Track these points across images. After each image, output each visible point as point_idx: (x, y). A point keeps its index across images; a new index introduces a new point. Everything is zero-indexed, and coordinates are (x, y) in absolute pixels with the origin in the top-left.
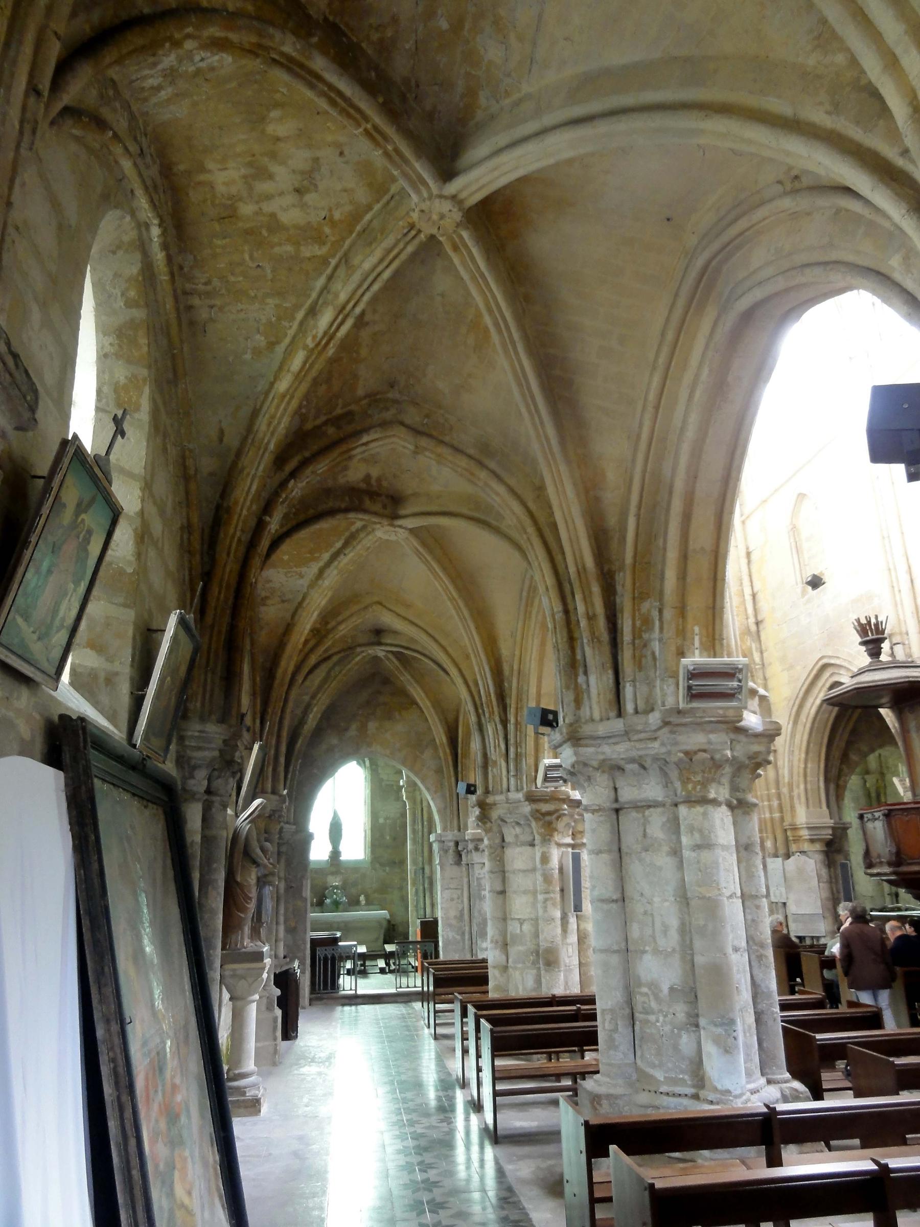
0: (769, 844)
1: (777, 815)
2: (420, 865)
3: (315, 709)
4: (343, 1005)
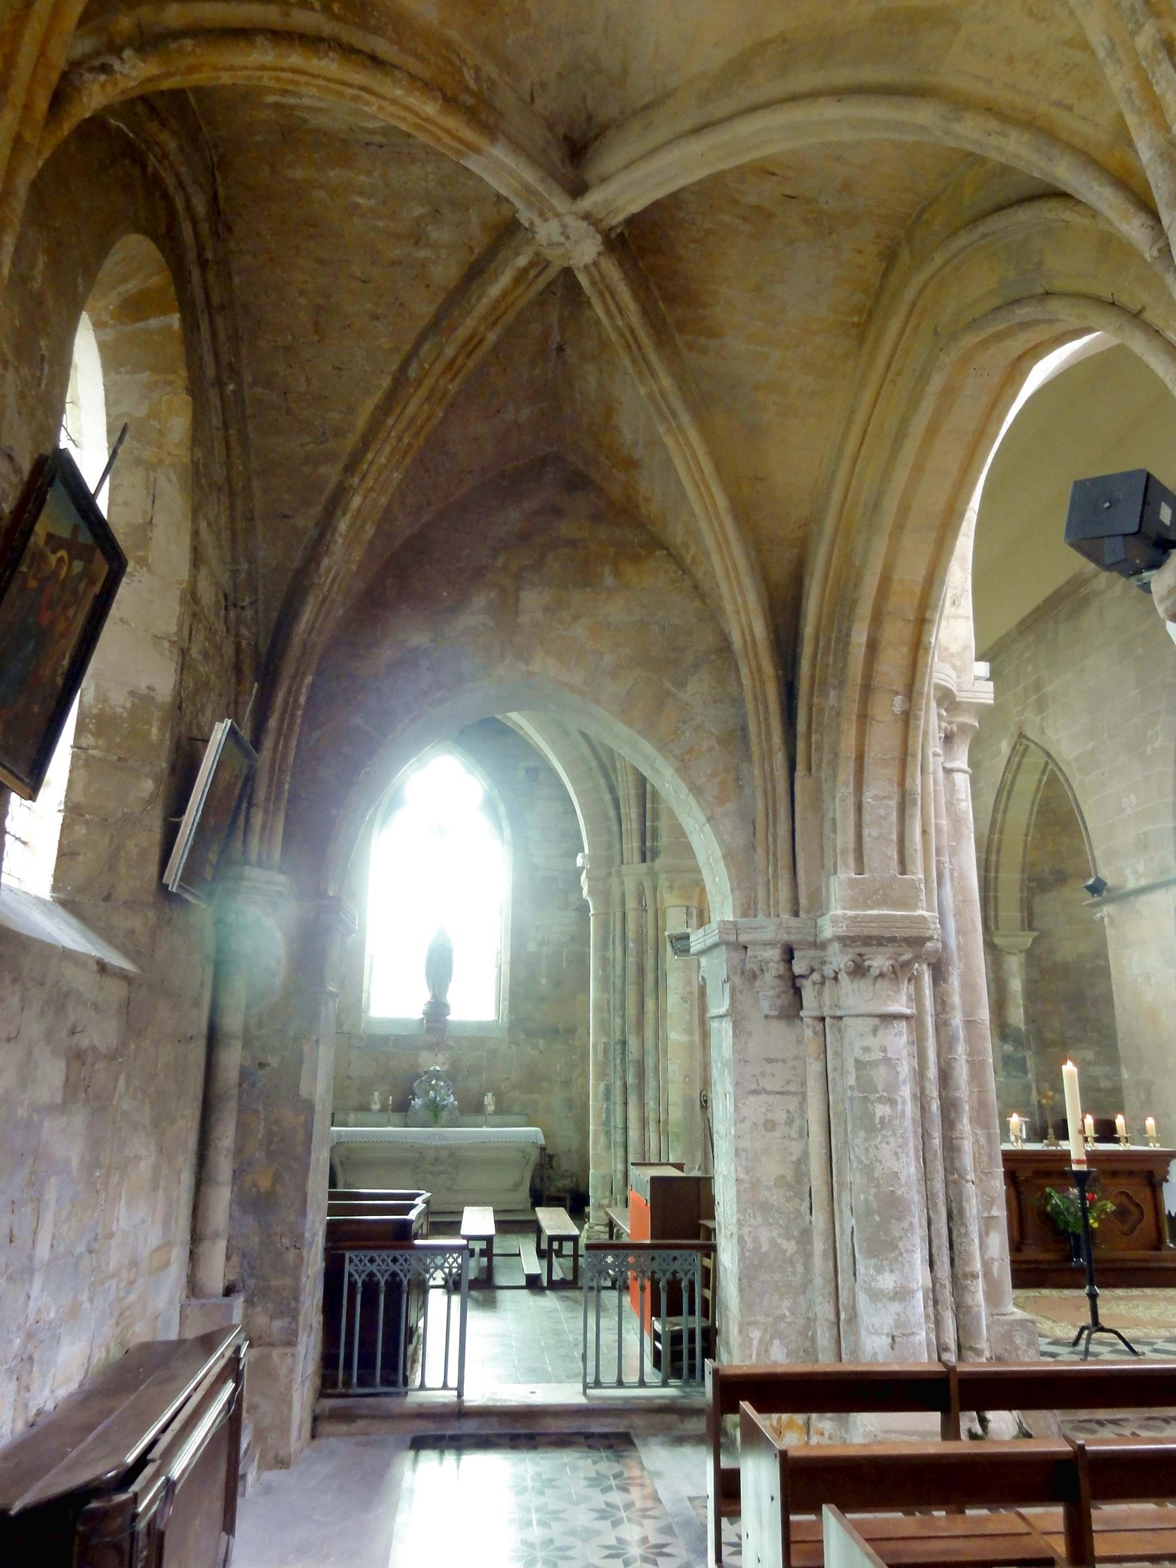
2: (618, 1036)
3: (356, 502)
4: (419, 1444)
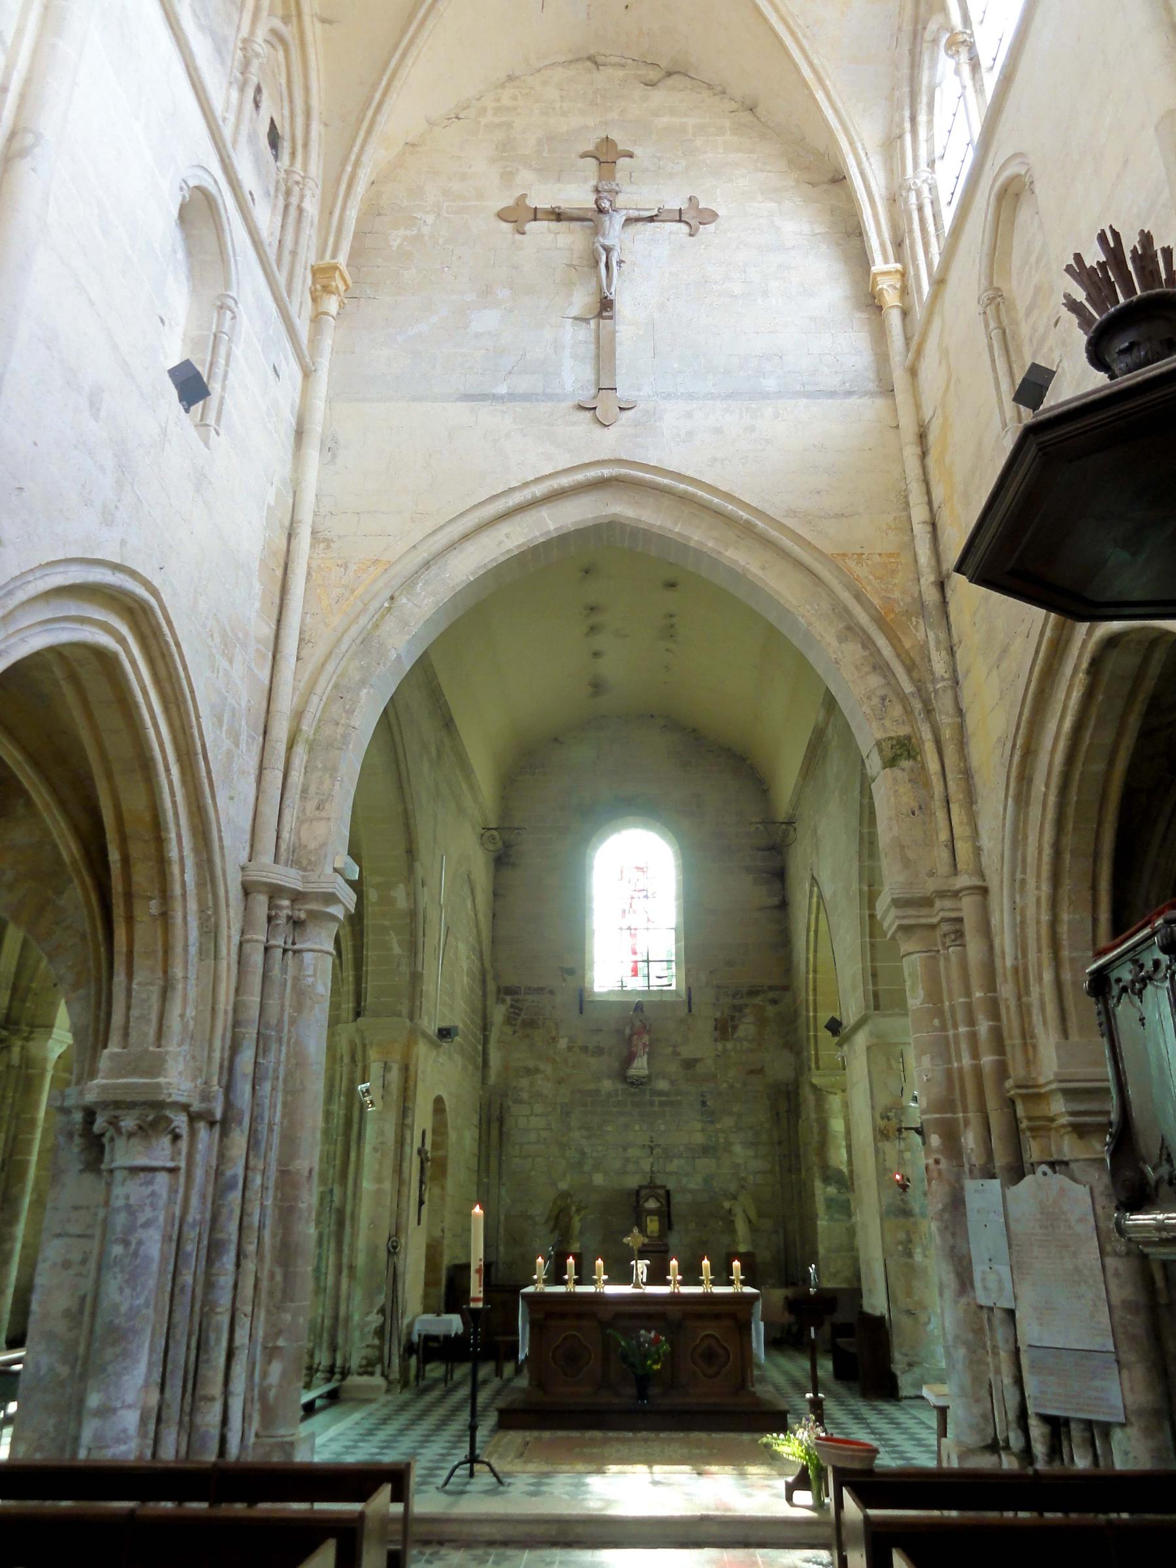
0: (970, 1140)
1: (988, 1060)
